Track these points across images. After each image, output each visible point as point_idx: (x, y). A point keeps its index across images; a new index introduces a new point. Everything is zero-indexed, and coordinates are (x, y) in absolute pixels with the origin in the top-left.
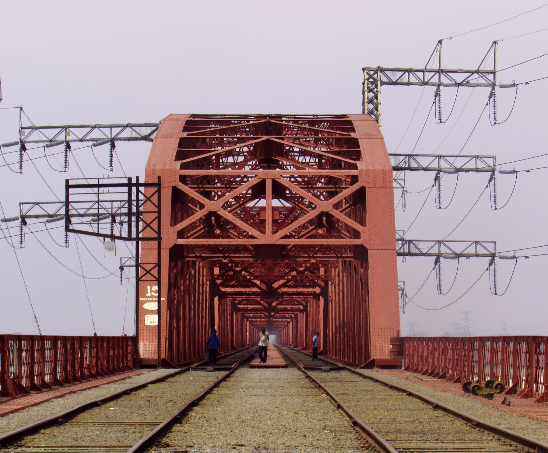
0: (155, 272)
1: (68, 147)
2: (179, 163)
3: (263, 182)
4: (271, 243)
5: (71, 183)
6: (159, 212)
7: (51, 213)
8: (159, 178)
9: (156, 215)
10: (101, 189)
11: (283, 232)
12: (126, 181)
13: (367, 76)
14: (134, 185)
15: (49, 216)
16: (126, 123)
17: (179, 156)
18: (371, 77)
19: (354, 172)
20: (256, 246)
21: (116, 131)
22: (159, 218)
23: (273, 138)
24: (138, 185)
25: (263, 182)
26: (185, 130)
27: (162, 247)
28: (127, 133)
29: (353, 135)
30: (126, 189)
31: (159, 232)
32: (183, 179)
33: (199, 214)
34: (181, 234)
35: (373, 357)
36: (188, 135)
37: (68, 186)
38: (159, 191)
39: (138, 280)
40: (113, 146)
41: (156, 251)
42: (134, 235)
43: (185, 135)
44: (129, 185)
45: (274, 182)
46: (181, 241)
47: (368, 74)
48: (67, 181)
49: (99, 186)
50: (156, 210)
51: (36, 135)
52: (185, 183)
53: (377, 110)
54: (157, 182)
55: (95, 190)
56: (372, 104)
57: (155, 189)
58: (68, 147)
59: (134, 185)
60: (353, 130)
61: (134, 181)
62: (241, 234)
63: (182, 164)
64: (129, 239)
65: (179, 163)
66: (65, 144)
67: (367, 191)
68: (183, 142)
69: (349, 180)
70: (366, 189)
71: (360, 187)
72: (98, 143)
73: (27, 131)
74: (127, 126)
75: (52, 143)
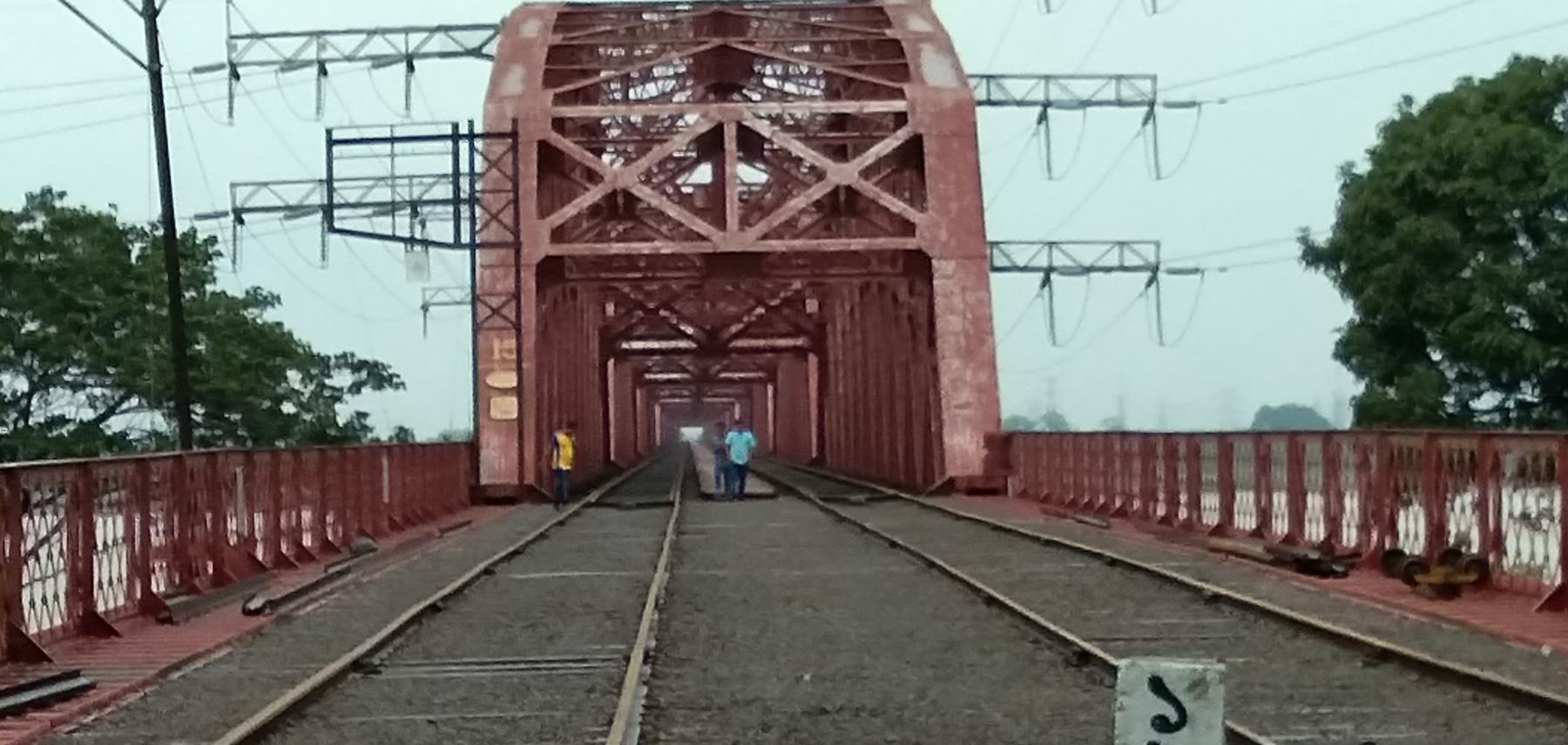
0: (510, 312)
5: (336, 135)
10: (398, 147)
12: (448, 130)
17: (551, 79)
19: (899, 105)
20: (706, 256)
22: (516, 201)
24: (471, 136)
26: (556, 29)
28: (438, 43)
31: (516, 232)
32: (559, 124)
36: (564, 39)
37: (331, 143)
40: (411, 68)
42: (465, 238)
43: (558, 39)
44: (455, 137)
48: (329, 132)
49: (393, 140)
55: (387, 147)
58: (323, 72)
61: (464, 130)
64: (457, 244)
68: (554, 53)
72: (380, 62)
75: (289, 65)
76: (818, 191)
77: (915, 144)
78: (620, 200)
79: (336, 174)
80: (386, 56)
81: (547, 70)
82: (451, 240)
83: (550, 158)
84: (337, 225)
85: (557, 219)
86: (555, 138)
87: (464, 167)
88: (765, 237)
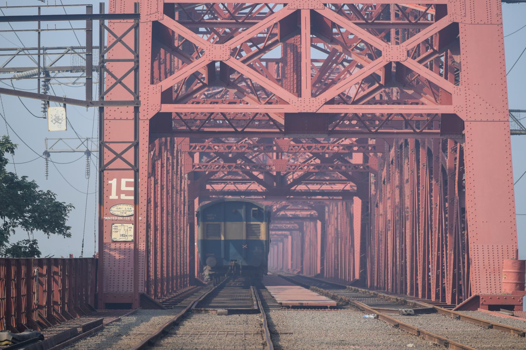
4: (311, 111)
9: (132, 65)
14: (96, 17)
25: (297, 14)
30: (83, 23)
38: (136, 27)
41: (133, 122)
44: (89, 17)
46: (167, 108)
59: (96, 17)
64: (88, 103)
67: (461, 30)
70: (460, 25)
71: (451, 23)
77: (454, 28)
82: (84, 98)
87: (96, 42)
88: (332, 102)
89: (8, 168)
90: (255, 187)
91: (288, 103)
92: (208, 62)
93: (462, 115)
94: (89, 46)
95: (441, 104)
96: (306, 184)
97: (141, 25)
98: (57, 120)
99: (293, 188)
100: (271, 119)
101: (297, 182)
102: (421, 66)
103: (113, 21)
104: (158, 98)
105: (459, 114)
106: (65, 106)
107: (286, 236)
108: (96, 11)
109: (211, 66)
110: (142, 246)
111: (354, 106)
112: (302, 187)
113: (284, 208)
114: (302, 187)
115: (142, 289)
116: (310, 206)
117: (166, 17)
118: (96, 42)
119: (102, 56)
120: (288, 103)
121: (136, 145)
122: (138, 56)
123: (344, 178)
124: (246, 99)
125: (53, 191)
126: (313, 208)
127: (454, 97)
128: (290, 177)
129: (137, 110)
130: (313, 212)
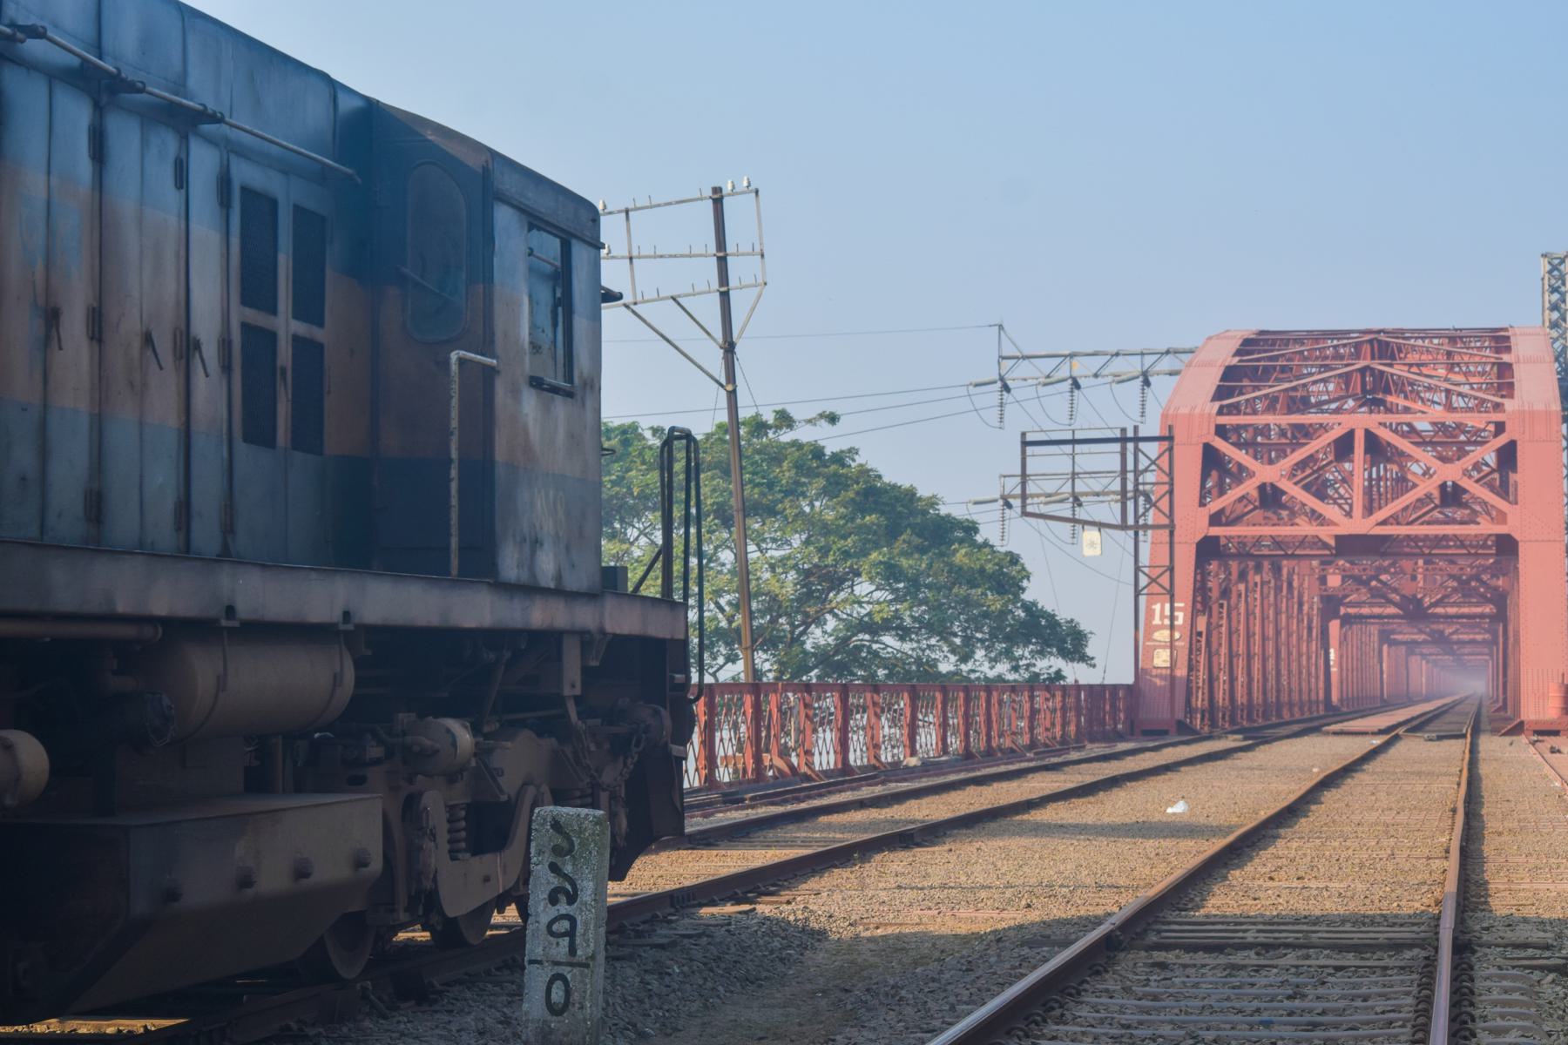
1: (1076, 385)
2: (1217, 405)
3: (1350, 435)
5: (1029, 438)
6: (1171, 484)
7: (1049, 491)
8: (1170, 428)
9: (1167, 487)
10: (1078, 448)
11: (1380, 515)
12: (1118, 434)
13: (1548, 267)
14: (1130, 440)
15: (1049, 495)
16: (1164, 349)
17: (1220, 393)
18: (1554, 268)
20: (1338, 538)
21: (1149, 360)
22: (1171, 492)
23: (1378, 366)
24: (1137, 439)
25: (1350, 435)
26: (1238, 353)
27: (1176, 539)
28: (1167, 363)
29: (1506, 358)
30: (1117, 447)
31: (1171, 516)
32: (1221, 431)
33: (1249, 487)
34: (1215, 519)
35: (1523, 717)
36: (1240, 361)
37: (1025, 444)
38: (1171, 449)
39: (1137, 594)
40: (1147, 383)
41: (1168, 546)
42: (1131, 521)
44: (1123, 440)
45: (1370, 437)
46: (1215, 531)
47: (1549, 263)
48: (1024, 434)
49: (1074, 442)
50: (1166, 479)
51: (1025, 368)
52: (1226, 438)
53: (1565, 320)
54: (1167, 434)
56: (1559, 311)
57: (1166, 444)
59: (1130, 440)
60: (1508, 349)
62: (1316, 517)
63: (1221, 408)
64: (1123, 526)
65: (1217, 405)
66: (1070, 381)
67: (1519, 448)
68: (1230, 373)
69: (1491, 428)
70: (1518, 443)
72: (1121, 380)
73: (1007, 364)
74: (1168, 352)
76: (1429, 487)
78: (1268, 488)
79: (1029, 471)
80: (1125, 374)
81: (1219, 386)
82: (1117, 520)
83: (1211, 459)
84: (1029, 509)
85: (1215, 505)
86: (1219, 443)
87: (1130, 466)
88: (1384, 523)
89: (1027, 596)
90: (1392, 610)
91: (1335, 524)
92: (1258, 484)
93: (1516, 536)
94: (1124, 471)
95: (1498, 523)
96: (1444, 607)
97: (1175, 447)
98: (1092, 544)
99: (1430, 611)
100: (1320, 540)
101: (1435, 604)
102: (1475, 485)
103: (1163, 443)
104: (1206, 520)
105: (1513, 534)
106: (1100, 530)
107: (1487, 661)
108: (1130, 434)
109: (1262, 488)
110: (1181, 672)
111: (1409, 527)
112: (1440, 610)
113: (1453, 633)
114: (1440, 610)
115: (1180, 715)
116: (1484, 629)
117: (1217, 439)
118: (1130, 466)
119: (1136, 479)
120: (1335, 524)
121: (1171, 569)
122: (1172, 479)
123: (1482, 600)
124: (1297, 521)
125: (1077, 619)
126: (1487, 631)
127: (1509, 518)
128: (1427, 599)
129: (1172, 534)
130: (1487, 636)
